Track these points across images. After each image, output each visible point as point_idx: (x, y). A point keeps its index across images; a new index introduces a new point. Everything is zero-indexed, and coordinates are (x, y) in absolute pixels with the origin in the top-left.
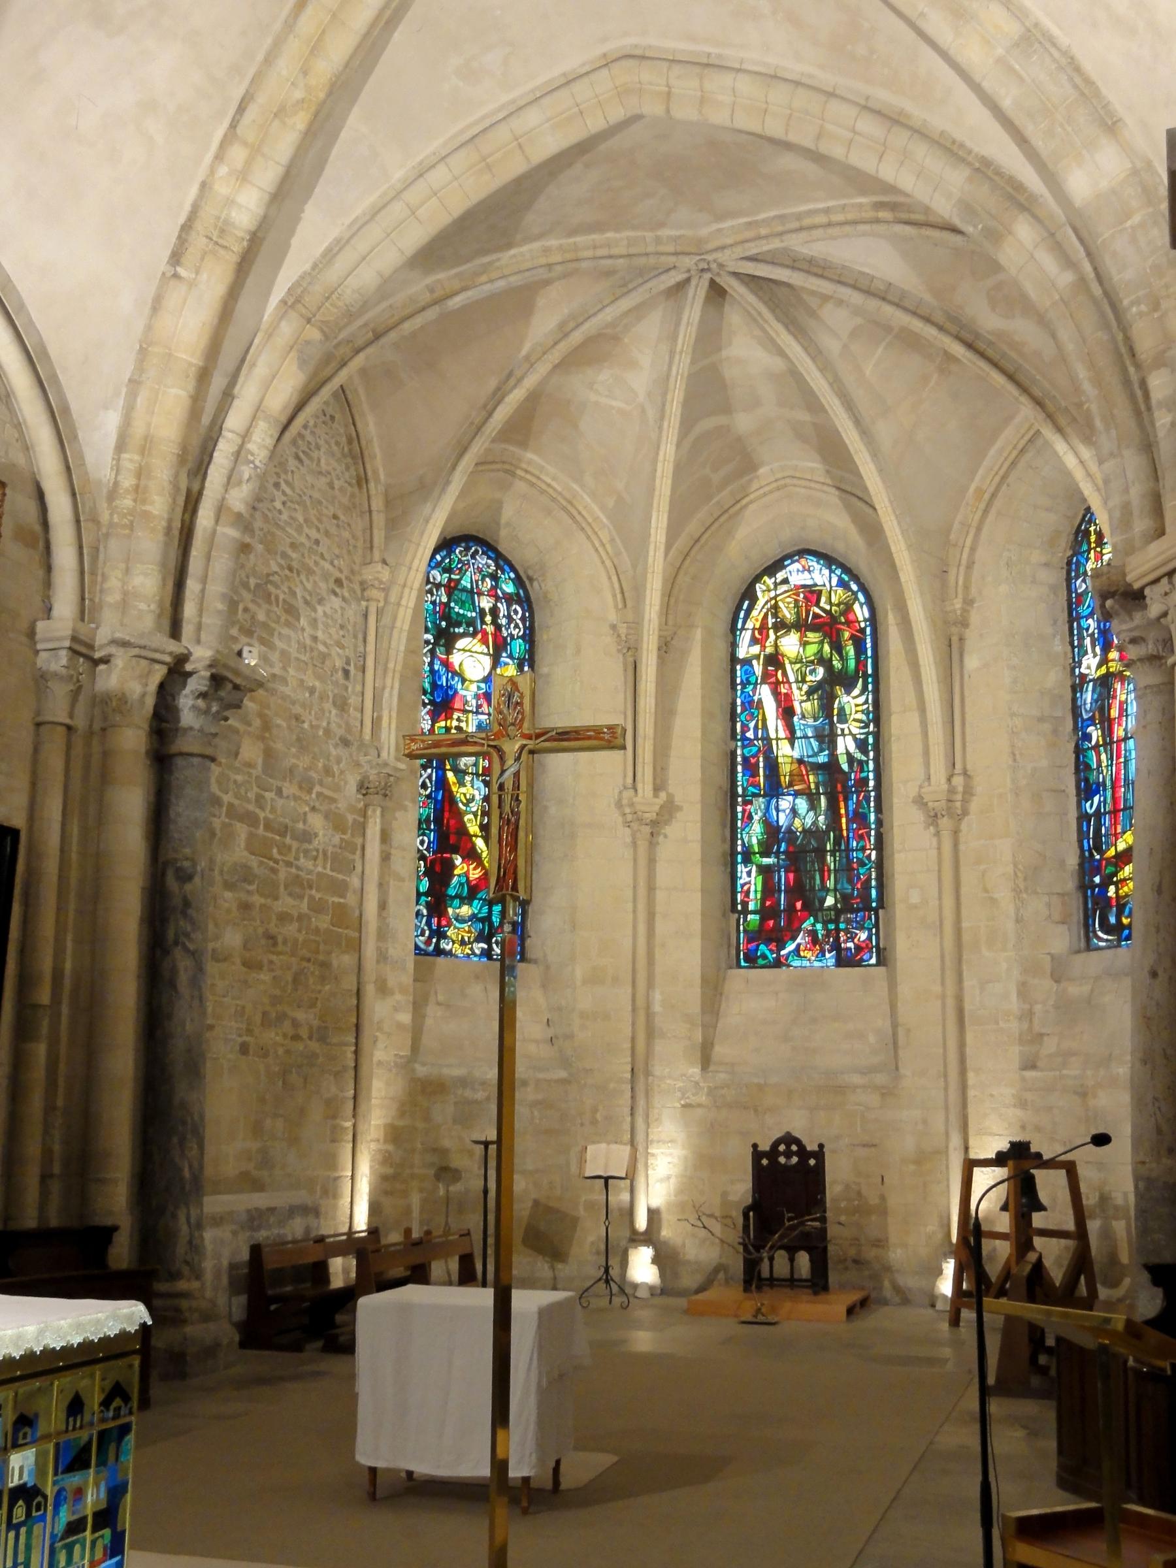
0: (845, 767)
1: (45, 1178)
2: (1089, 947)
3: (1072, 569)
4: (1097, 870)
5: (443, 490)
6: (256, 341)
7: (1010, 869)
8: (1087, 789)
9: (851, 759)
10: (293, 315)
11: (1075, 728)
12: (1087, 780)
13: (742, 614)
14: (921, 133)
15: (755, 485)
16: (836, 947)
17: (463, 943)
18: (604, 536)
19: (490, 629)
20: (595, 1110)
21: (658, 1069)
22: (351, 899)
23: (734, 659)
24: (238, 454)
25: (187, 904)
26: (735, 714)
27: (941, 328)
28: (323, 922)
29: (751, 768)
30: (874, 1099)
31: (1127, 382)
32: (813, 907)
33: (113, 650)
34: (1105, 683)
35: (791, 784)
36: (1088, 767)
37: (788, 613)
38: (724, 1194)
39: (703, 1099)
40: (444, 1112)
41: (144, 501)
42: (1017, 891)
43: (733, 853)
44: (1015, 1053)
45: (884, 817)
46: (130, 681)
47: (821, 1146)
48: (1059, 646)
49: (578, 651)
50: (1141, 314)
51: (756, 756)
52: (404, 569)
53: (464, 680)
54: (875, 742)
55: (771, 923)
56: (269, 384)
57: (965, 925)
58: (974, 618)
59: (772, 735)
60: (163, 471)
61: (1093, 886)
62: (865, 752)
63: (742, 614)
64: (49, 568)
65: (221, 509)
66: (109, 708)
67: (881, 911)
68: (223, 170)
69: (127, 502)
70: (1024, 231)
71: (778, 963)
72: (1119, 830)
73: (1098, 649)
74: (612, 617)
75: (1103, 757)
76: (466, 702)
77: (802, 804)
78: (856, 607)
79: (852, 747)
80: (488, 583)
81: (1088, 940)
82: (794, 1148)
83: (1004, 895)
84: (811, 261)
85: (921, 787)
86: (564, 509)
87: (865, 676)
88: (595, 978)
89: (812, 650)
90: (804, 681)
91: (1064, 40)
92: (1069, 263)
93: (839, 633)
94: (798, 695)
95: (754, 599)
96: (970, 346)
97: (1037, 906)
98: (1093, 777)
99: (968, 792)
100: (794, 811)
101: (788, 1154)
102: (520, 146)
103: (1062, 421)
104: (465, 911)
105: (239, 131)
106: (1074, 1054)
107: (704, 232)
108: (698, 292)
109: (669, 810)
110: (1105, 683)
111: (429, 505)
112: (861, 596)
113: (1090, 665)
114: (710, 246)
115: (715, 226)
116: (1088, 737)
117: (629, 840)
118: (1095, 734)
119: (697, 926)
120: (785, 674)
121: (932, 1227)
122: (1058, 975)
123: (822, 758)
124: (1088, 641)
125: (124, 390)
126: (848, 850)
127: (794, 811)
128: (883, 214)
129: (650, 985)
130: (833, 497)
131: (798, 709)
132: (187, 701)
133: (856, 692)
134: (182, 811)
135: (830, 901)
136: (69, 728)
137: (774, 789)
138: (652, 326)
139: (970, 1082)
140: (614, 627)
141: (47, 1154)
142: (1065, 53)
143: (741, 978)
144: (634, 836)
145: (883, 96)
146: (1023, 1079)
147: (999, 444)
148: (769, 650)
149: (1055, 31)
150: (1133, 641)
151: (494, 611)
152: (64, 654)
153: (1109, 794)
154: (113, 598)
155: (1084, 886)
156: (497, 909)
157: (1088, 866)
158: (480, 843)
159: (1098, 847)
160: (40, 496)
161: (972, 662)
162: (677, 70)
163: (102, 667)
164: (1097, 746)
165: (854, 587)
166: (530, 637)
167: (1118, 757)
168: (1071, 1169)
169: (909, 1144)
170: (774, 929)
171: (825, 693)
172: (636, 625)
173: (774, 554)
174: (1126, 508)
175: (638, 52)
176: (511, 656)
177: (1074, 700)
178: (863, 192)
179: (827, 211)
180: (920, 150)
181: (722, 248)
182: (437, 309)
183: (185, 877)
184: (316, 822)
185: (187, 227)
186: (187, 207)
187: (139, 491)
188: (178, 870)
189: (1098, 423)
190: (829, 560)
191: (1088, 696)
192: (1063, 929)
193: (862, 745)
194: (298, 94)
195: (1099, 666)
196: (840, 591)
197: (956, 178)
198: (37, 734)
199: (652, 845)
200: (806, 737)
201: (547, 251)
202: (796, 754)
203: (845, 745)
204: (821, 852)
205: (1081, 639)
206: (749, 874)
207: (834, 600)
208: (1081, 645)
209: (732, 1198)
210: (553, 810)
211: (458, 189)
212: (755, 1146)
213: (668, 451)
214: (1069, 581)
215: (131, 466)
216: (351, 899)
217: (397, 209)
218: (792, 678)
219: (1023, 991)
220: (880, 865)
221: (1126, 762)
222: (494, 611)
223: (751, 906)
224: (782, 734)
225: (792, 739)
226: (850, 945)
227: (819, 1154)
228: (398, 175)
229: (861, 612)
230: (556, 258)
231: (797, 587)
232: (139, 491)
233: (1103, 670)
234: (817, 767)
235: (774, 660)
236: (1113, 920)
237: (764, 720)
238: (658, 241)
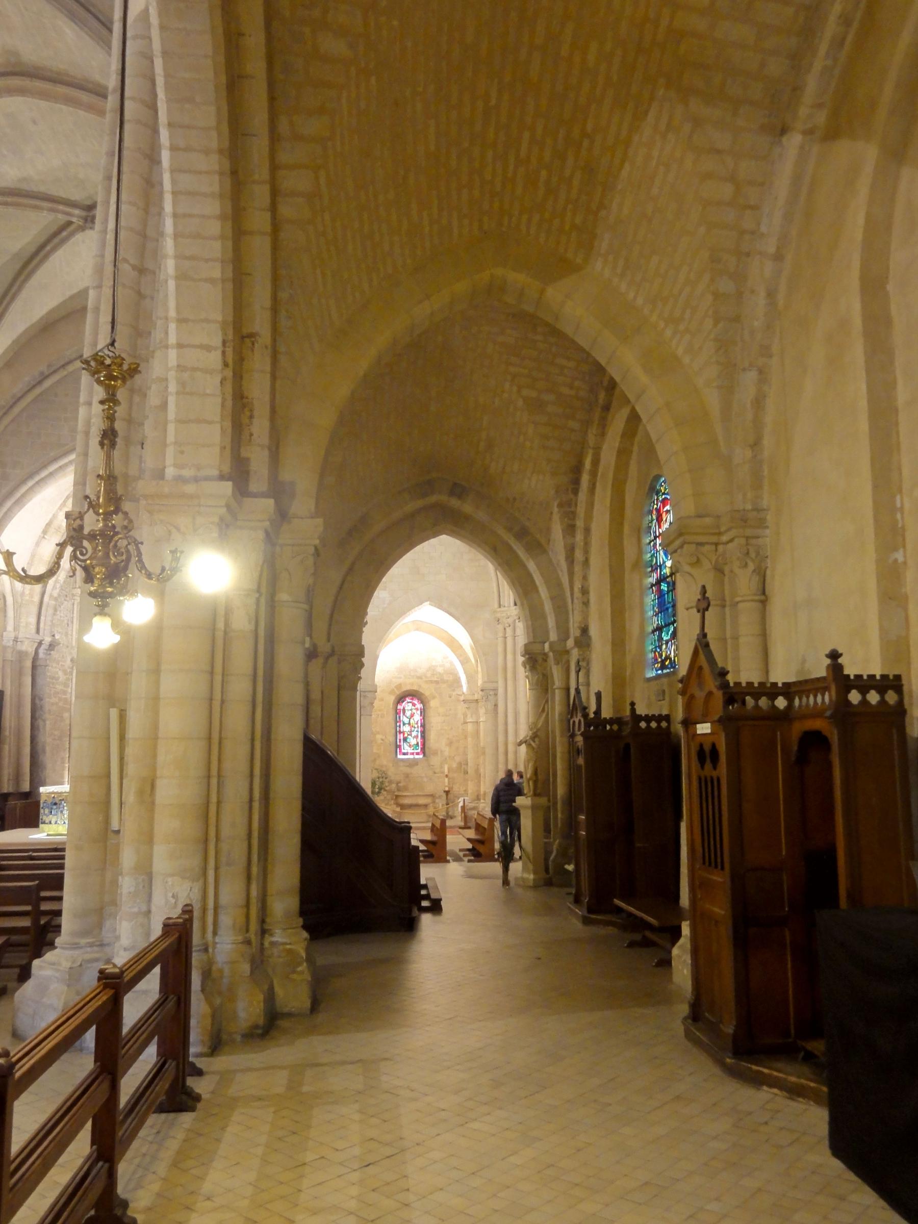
1: (9, 780)
22: (68, 696)
25: (41, 707)
28: (61, 704)
46: (28, 647)
64: (5, 616)
65: (51, 596)
66: (21, 655)
134: (39, 681)
141: (9, 774)
160: (4, 597)
183: (41, 700)
184: (60, 673)
185: (49, 525)
216: (68, 696)
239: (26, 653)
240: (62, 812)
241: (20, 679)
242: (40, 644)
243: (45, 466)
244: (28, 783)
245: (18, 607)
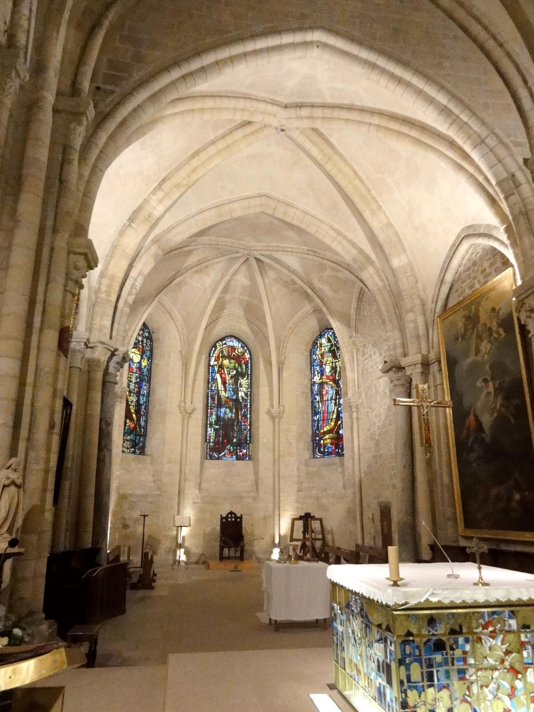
0: (241, 401)
1: (66, 530)
2: (314, 457)
3: (312, 352)
4: (317, 436)
5: (151, 303)
6: (142, 250)
7: (295, 434)
8: (315, 412)
9: (243, 398)
10: (156, 245)
11: (312, 396)
12: (315, 410)
13: (212, 352)
14: (345, 238)
15: (223, 315)
16: (236, 454)
17: (127, 448)
18: (180, 323)
19: (141, 347)
20: (167, 504)
21: (186, 491)
23: (209, 365)
24: (132, 285)
26: (210, 381)
27: (306, 284)
29: (213, 399)
30: (250, 501)
31: (396, 313)
32: (230, 442)
33: (98, 344)
34: (321, 385)
35: (225, 405)
36: (315, 407)
37: (225, 353)
38: (205, 531)
39: (199, 501)
40: (126, 506)
41: (109, 296)
42: (297, 440)
43: (207, 424)
44: (295, 487)
45: (253, 416)
47: (242, 515)
48: (308, 373)
49: (169, 357)
50: (407, 298)
51: (215, 395)
52: (134, 326)
53: (133, 362)
54: (250, 394)
55: (217, 446)
56: (145, 265)
57: (281, 449)
58: (286, 362)
59: (220, 389)
60: (117, 288)
61: (316, 440)
62: (247, 397)
63: (212, 352)
65: (126, 302)
66: (91, 364)
67: (250, 444)
68: (154, 198)
69: (104, 295)
70: (371, 270)
71: (218, 458)
72: (325, 425)
73: (319, 375)
74: (180, 348)
75: (320, 405)
76: (133, 370)
77: (228, 411)
78: (246, 354)
79: (243, 395)
80: (141, 332)
81: (314, 455)
82: (233, 515)
83: (293, 441)
84: (276, 259)
85: (268, 409)
86: (169, 313)
87: (248, 374)
88: (169, 462)
89: (233, 365)
90: (229, 374)
91: (395, 227)
92: (382, 280)
93: (241, 361)
94: (228, 378)
95: (216, 348)
96: (312, 290)
98: (317, 410)
99: (284, 411)
100: (225, 413)
101: (231, 518)
102: (231, 212)
103: (333, 315)
104: (129, 437)
105: (162, 187)
106: (315, 487)
107: (250, 245)
108: (242, 260)
109: (194, 410)
110: (321, 385)
111: (144, 308)
112: (247, 351)
113: (317, 379)
114: (252, 249)
115: (255, 244)
116: (316, 399)
117: (181, 418)
118: (318, 398)
119: (199, 446)
120: (224, 371)
121: (267, 539)
122: (306, 465)
123: (234, 397)
124: (316, 373)
125: (104, 258)
126: (241, 425)
127: (225, 413)
128: (310, 253)
129: (186, 464)
130: (245, 322)
131: (228, 382)
132: (112, 365)
133: (245, 379)
135: (235, 440)
136: (80, 369)
137: (220, 405)
138: (219, 266)
139: (281, 496)
140: (180, 351)
141: (67, 523)
142: (395, 230)
143: (209, 463)
144: (183, 416)
145: (336, 226)
146: (298, 494)
147: (297, 316)
148: (220, 364)
149: (394, 224)
150: (398, 380)
151: (142, 341)
152: (83, 344)
153: (322, 415)
154: (96, 327)
155: (313, 440)
156: (138, 437)
157: (314, 435)
158: (134, 415)
159: (318, 429)
161: (285, 375)
162: (280, 203)
163: (88, 349)
164: (318, 402)
165: (246, 348)
167: (325, 405)
168: (321, 520)
169: (261, 514)
171: (235, 378)
172: (190, 352)
173: (224, 335)
174: (395, 345)
175: (269, 196)
176: (146, 356)
177: (311, 388)
178: (305, 246)
179: (292, 248)
180: (345, 242)
181: (257, 250)
182: (180, 250)
185: (136, 213)
186: (137, 205)
187: (108, 293)
188: (107, 421)
189: (387, 323)
190: (239, 340)
191: (316, 388)
192: (308, 451)
193: (246, 394)
194: (185, 182)
195: (320, 380)
196: (241, 349)
197: (354, 252)
198: (70, 370)
199: (188, 419)
200: (229, 391)
201: (211, 240)
202: (227, 396)
203: (241, 394)
205: (314, 372)
206: (211, 430)
207: (240, 351)
208: (314, 373)
209: (207, 532)
210: (157, 407)
211: (209, 219)
212: (221, 515)
213: (213, 302)
214: (311, 355)
215: (106, 284)
217: (193, 221)
218: (226, 373)
219: (298, 469)
220: (250, 430)
221: (328, 406)
222: (142, 341)
223: (211, 441)
224: (223, 389)
225: (225, 390)
226: (241, 454)
227: (241, 518)
228: (194, 211)
229: (247, 356)
230: (213, 242)
231: (229, 346)
232: (108, 293)
233: (321, 381)
234: (232, 400)
235: (221, 367)
236: (322, 450)
237: (217, 384)
238: (239, 244)
239: (97, 362)
240: (462, 673)
241: (87, 396)
242: (113, 354)
243: (198, 54)
244: (90, 535)
245: (93, 306)
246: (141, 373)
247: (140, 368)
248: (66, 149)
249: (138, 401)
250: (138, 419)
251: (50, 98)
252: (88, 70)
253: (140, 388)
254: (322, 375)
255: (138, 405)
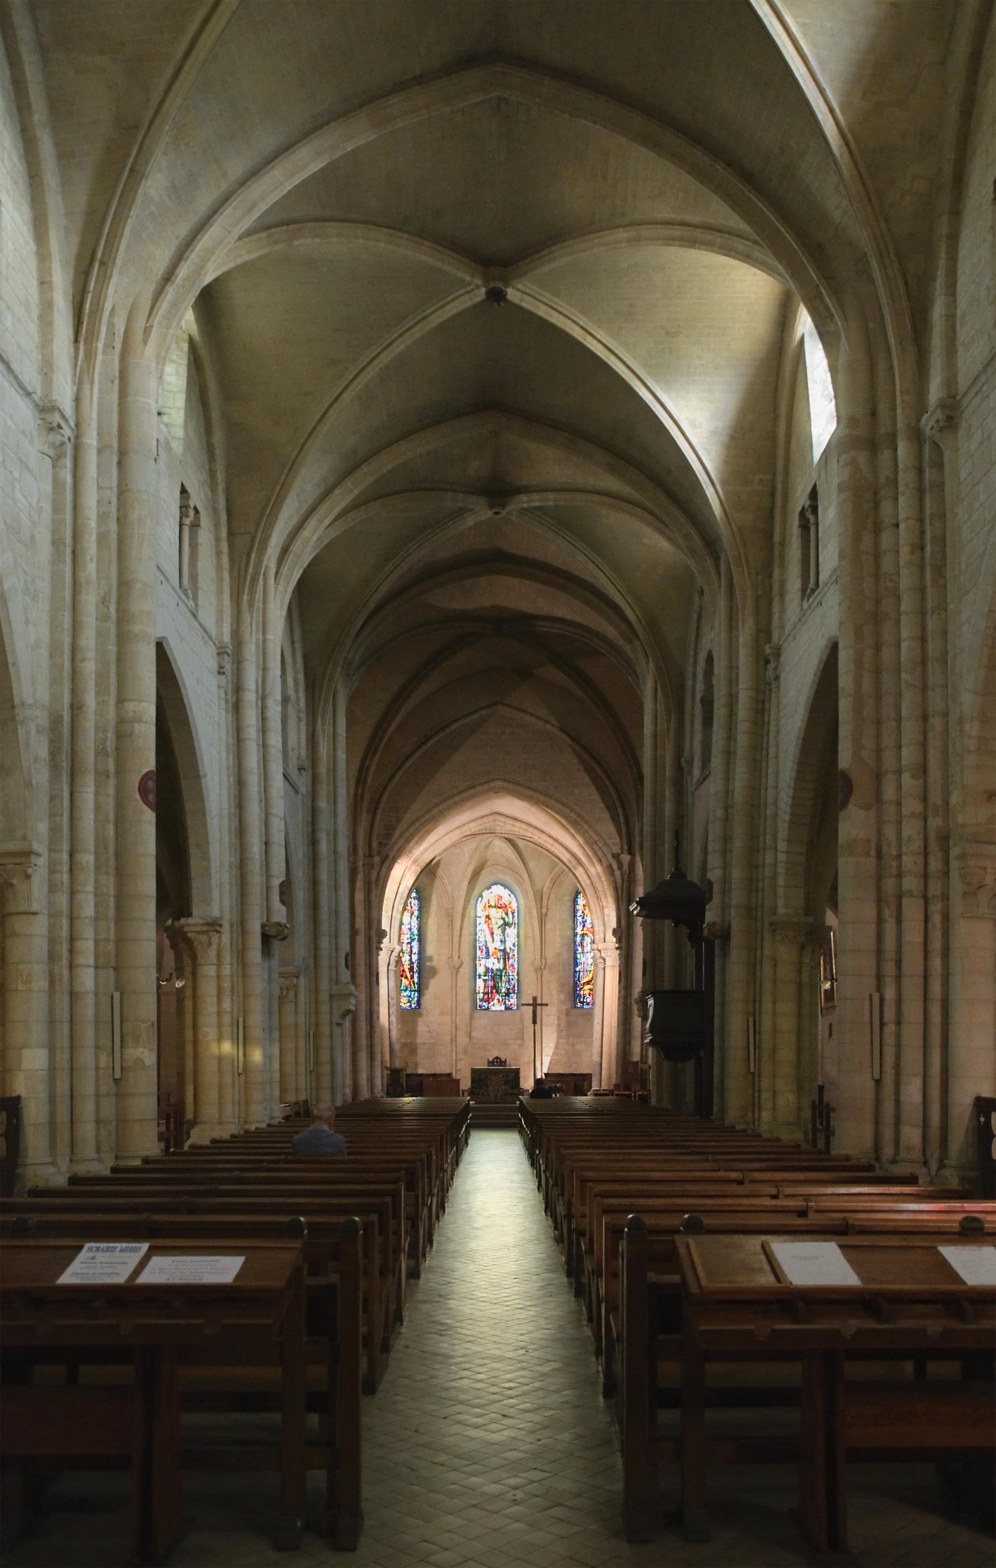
2: (575, 1007)
23: (476, 916)
30: (516, 1047)
94: (495, 927)
97: (562, 997)
109: (462, 964)
110: (583, 935)
123: (502, 948)
135: (503, 990)
137: (488, 955)
166: (420, 909)
170: (488, 998)
190: (506, 887)
193: (514, 945)
203: (509, 945)
204: (501, 976)
219: (559, 1018)
235: (488, 917)
246: (412, 934)
247: (410, 929)
248: (369, 883)
249: (411, 960)
250: (412, 977)
251: (360, 863)
252: (374, 837)
253: (411, 948)
254: (584, 926)
255: (412, 963)
